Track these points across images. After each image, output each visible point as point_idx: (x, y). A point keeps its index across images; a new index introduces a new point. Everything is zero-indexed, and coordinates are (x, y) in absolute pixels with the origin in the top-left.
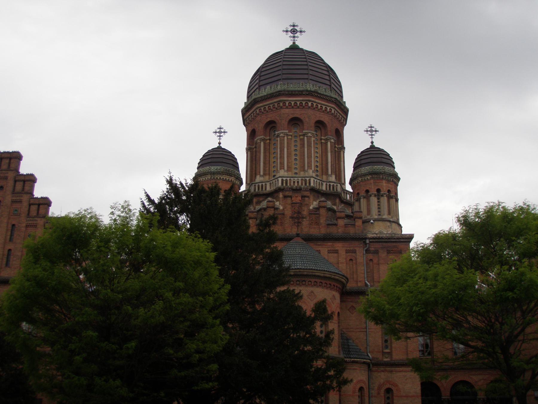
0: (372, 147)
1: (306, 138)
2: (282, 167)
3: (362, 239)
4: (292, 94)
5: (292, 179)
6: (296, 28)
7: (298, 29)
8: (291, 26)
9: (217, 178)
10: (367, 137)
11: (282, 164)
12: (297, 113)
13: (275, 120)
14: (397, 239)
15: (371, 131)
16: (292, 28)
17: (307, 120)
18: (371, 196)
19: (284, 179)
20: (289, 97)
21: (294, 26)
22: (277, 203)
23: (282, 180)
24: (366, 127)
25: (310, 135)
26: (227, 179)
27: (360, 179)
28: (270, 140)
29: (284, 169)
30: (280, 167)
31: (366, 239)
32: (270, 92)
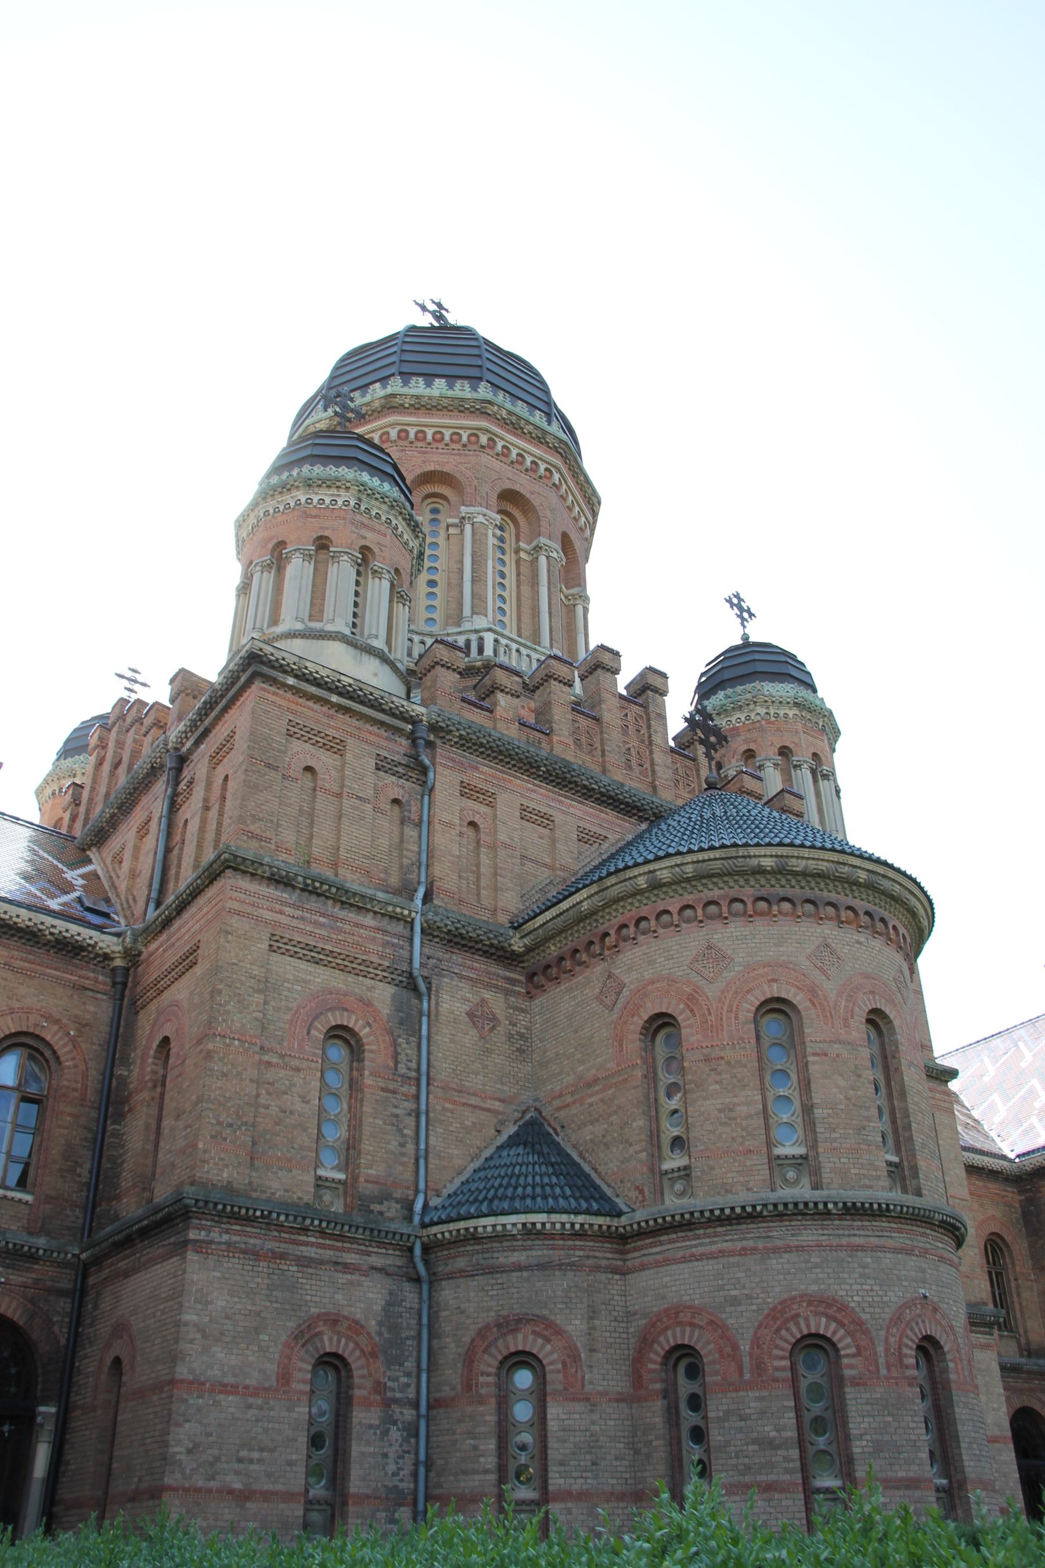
1: (543, 560)
4: (514, 425)
5: (524, 651)
6: (443, 312)
8: (433, 302)
9: (378, 516)
12: (523, 484)
13: (457, 475)
15: (741, 609)
16: (435, 308)
17: (548, 513)
19: (504, 641)
20: (508, 431)
21: (439, 305)
23: (496, 641)
24: (728, 593)
25: (555, 555)
26: (406, 537)
29: (486, 616)
32: (450, 393)
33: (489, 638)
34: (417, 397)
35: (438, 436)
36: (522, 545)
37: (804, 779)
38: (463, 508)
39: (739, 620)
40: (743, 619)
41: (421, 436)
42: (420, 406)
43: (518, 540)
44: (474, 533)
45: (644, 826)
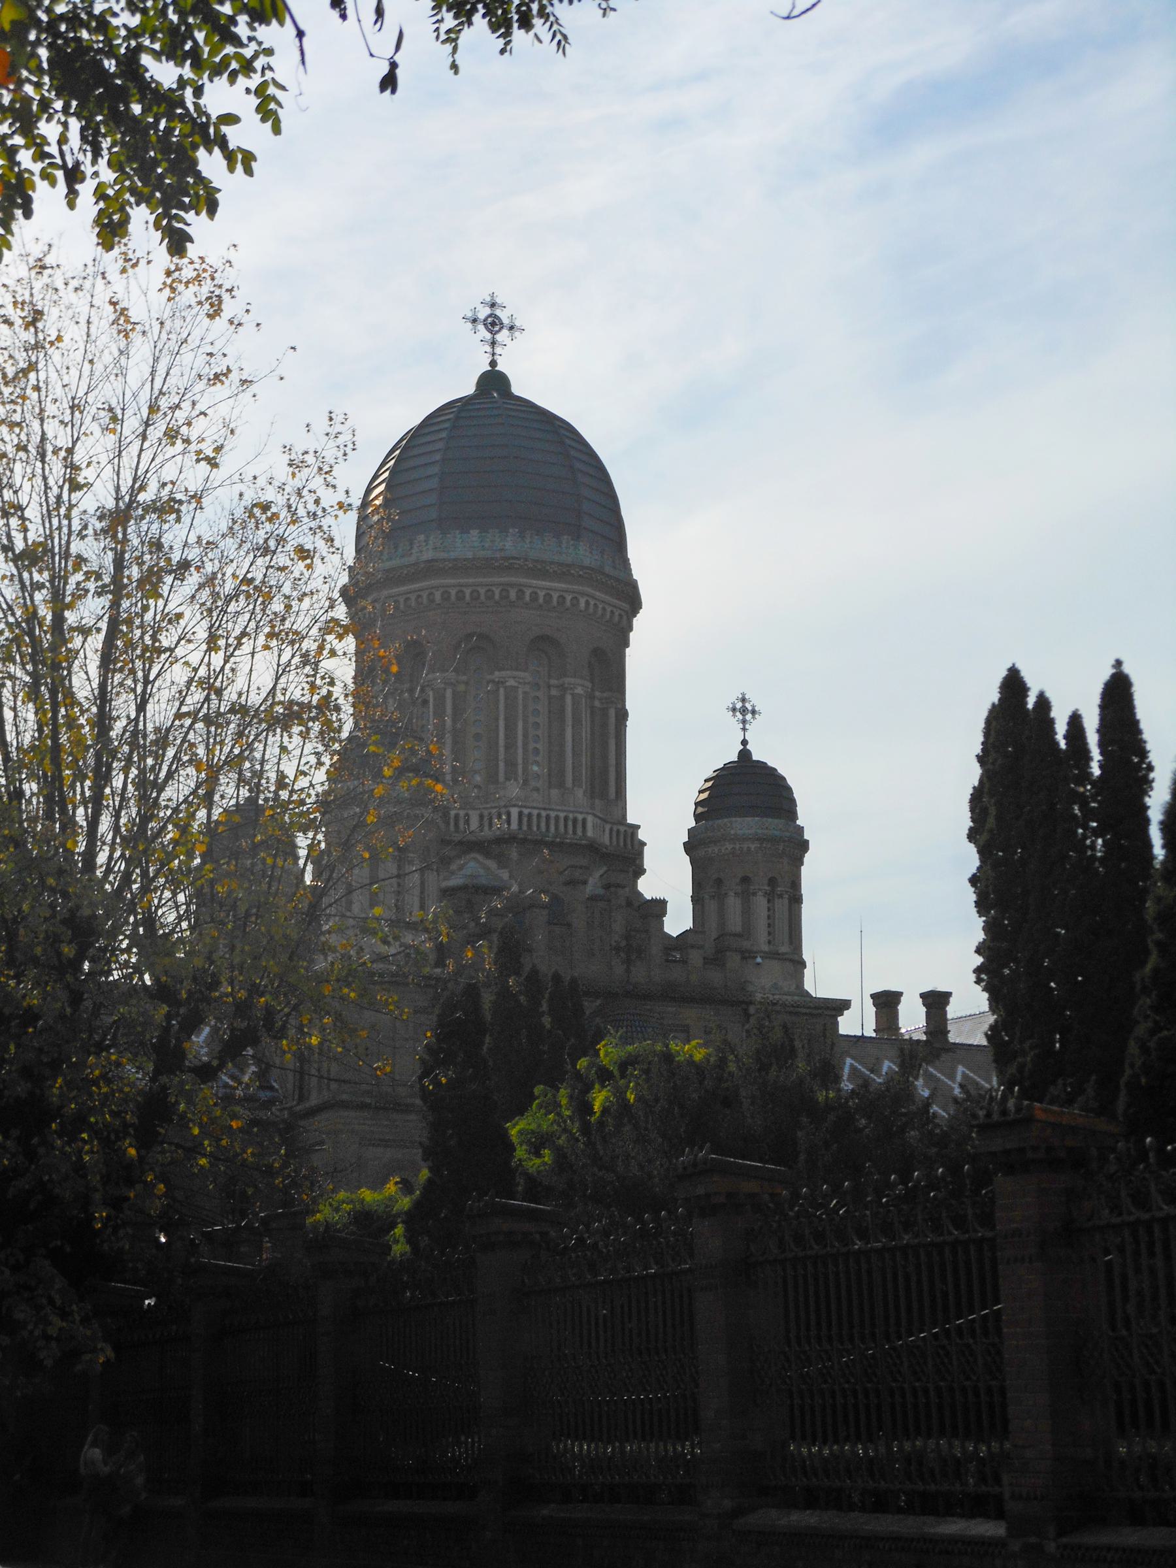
0: (745, 754)
2: (511, 774)
3: (743, 1002)
4: (540, 570)
7: (503, 315)
10: (734, 722)
11: (511, 764)
14: (816, 1008)
15: (744, 711)
16: (488, 311)
18: (754, 894)
19: (526, 811)
21: (493, 305)
22: (505, 875)
23: (520, 814)
24: (732, 698)
25: (579, 690)
27: (729, 846)
28: (467, 683)
29: (516, 780)
30: (506, 772)
31: (751, 1003)
33: (514, 812)
34: (455, 560)
35: (475, 594)
36: (553, 682)
37: (760, 902)
38: (497, 673)
39: (741, 726)
40: (744, 722)
41: (460, 596)
42: (460, 567)
43: (550, 677)
44: (506, 698)
45: (598, 1002)
